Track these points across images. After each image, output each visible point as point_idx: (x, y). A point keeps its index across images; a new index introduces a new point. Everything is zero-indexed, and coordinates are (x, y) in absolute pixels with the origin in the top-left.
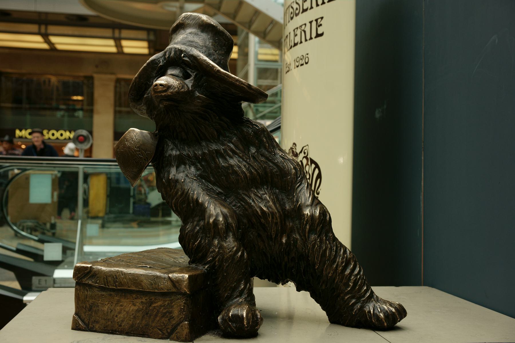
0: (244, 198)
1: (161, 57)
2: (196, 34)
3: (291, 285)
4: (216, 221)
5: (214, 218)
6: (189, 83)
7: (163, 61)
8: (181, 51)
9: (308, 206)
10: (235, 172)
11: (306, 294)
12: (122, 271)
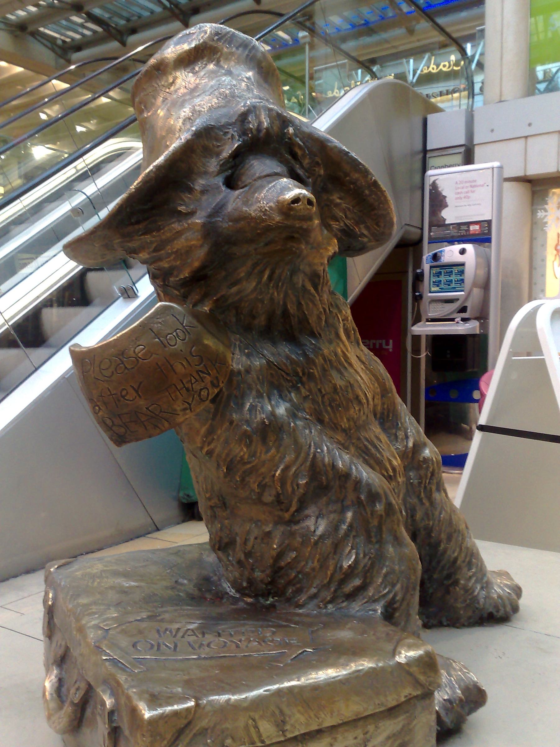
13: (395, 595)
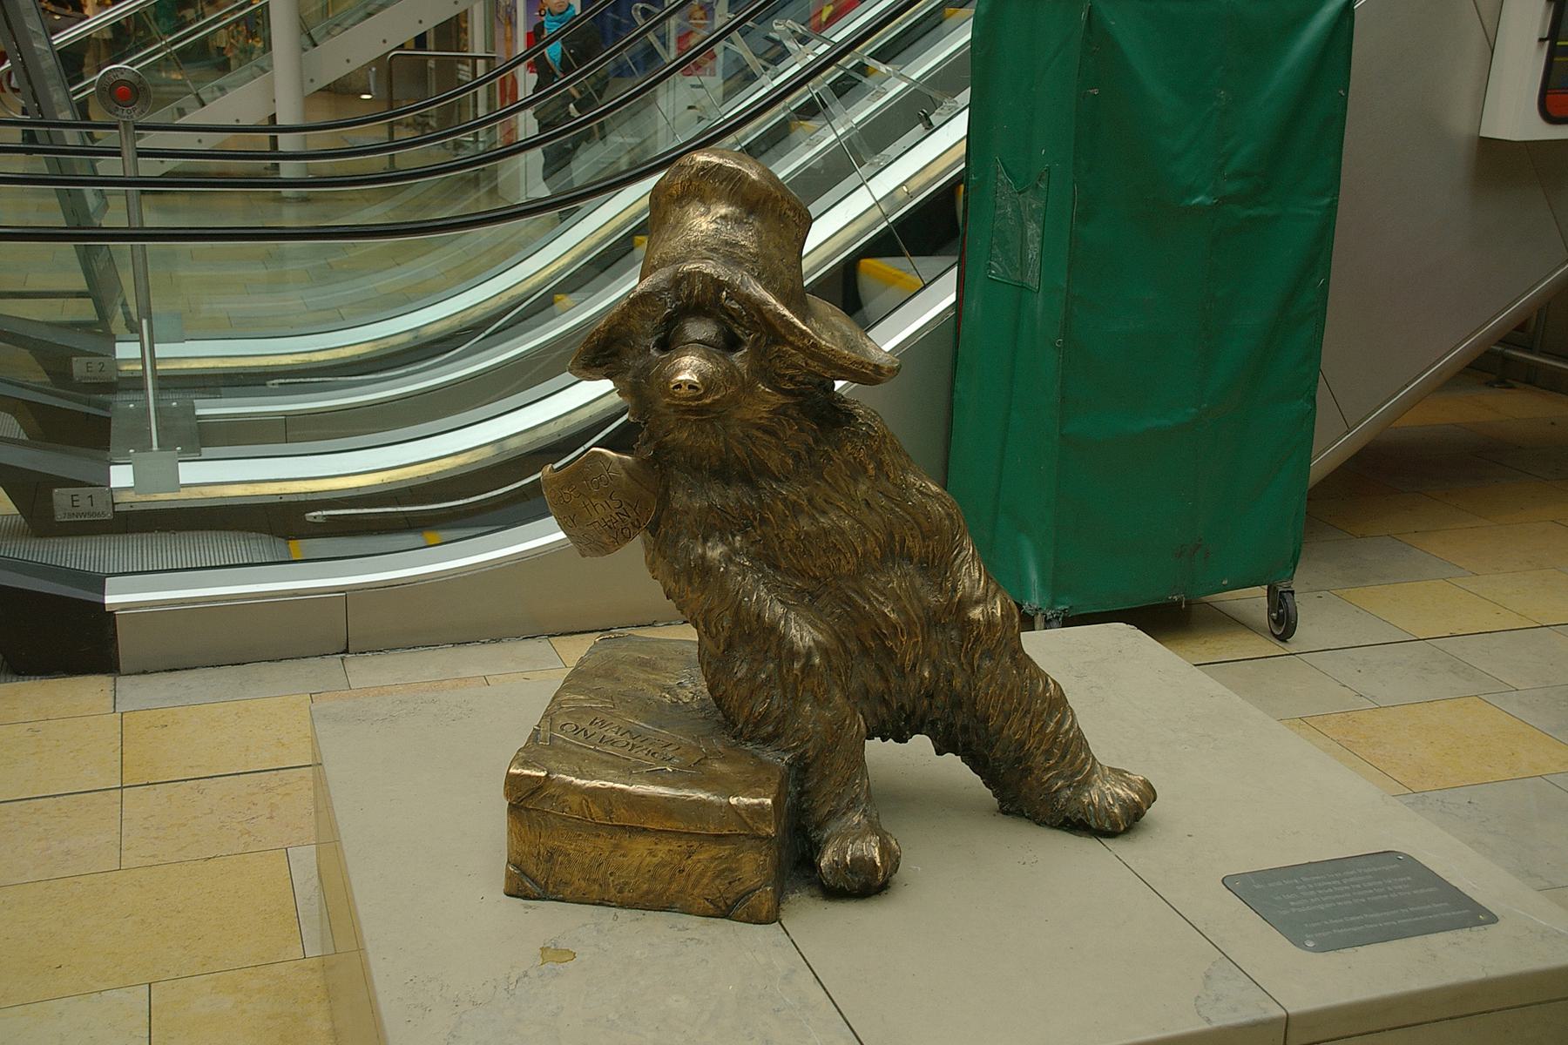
0: (849, 597)
2: (738, 221)
3: (921, 743)
4: (808, 668)
8: (719, 285)
9: (977, 602)
11: (952, 759)
12: (622, 790)
13: (806, 752)
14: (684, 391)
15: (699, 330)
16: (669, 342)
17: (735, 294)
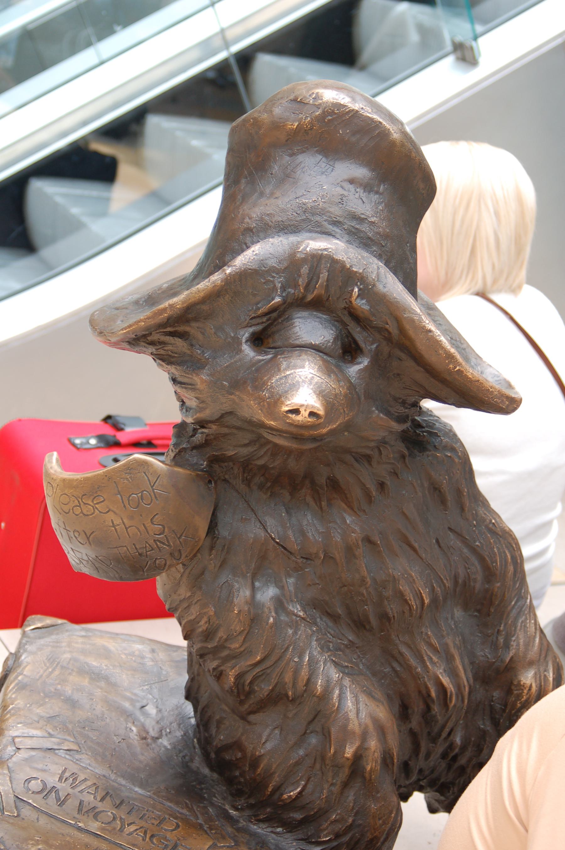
1: (278, 271)
2: (368, 187)
5: (357, 744)
6: (354, 370)
7: (283, 288)
9: (531, 663)
10: (401, 595)
14: (303, 417)
15: (311, 329)
16: (269, 335)
17: (369, 291)
